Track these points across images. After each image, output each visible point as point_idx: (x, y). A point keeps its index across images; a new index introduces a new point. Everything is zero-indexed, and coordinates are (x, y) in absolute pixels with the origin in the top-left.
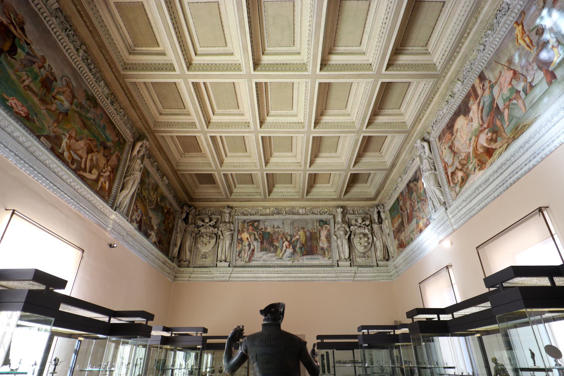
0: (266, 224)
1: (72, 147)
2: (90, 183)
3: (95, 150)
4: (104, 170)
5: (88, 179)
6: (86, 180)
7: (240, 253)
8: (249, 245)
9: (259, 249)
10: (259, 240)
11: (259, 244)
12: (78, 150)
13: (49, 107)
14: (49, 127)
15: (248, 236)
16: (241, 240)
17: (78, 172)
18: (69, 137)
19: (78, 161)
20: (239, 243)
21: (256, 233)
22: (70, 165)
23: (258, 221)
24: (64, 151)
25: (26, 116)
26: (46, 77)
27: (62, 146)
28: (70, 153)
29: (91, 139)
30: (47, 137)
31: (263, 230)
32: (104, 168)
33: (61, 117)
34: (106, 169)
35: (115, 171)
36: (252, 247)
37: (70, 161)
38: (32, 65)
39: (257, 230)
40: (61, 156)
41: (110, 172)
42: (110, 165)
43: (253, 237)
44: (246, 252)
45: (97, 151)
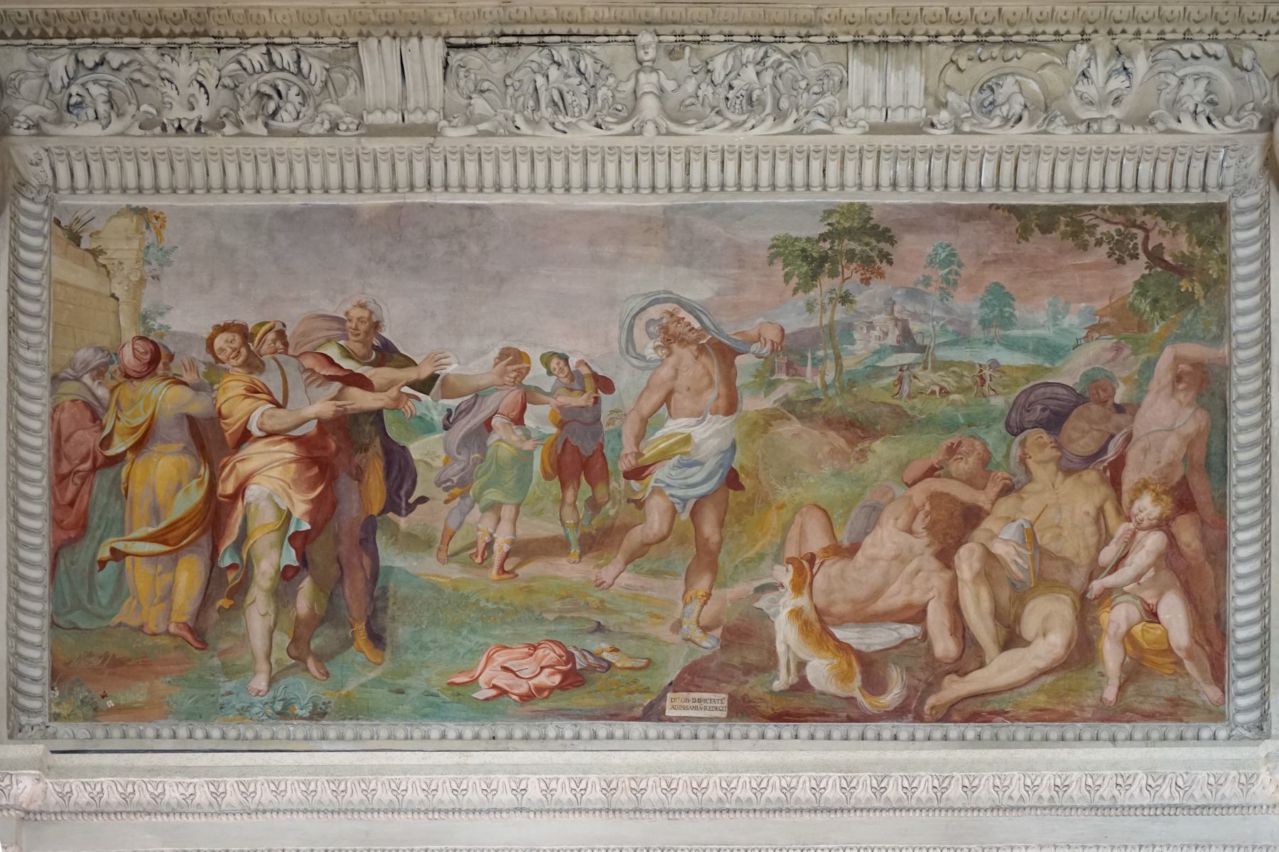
1: (840, 608)
2: (1042, 701)
3: (982, 499)
4: (1108, 554)
5: (1011, 688)
6: (994, 704)
12: (877, 594)
13: (635, 536)
14: (677, 627)
17: (931, 701)
18: (799, 571)
19: (906, 642)
22: (865, 702)
24: (802, 665)
25: (565, 675)
26: (561, 425)
27: (780, 648)
28: (843, 648)
29: (935, 458)
30: (692, 678)
32: (1105, 538)
33: (709, 529)
34: (1122, 529)
35: (1202, 495)
37: (855, 688)
38: (483, 448)
40: (795, 702)
41: (1163, 524)
42: (1143, 487)
45: (1007, 490)
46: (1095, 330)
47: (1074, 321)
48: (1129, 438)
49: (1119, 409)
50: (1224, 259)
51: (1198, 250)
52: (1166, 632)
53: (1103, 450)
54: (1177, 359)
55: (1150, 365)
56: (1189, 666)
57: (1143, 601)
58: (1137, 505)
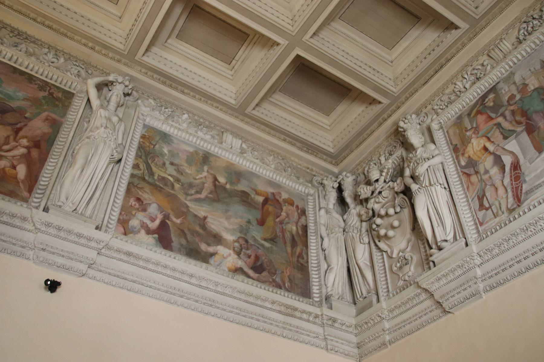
0: (517, 78)
7: (481, 198)
8: (498, 161)
9: (532, 151)
10: (519, 129)
11: (525, 137)
15: (483, 142)
16: (472, 163)
20: (468, 175)
21: (500, 120)
23: (493, 89)
31: (518, 97)
32: (7, 143)
34: (13, 144)
36: (507, 160)
39: (501, 111)
43: (497, 135)
44: (498, 184)
46: (25, 99)
47: (20, 94)
48: (26, 125)
49: (26, 118)
50: (70, 103)
51: (63, 98)
52: (17, 173)
53: (17, 124)
54: (48, 116)
55: (39, 114)
56: (21, 184)
57: (12, 163)
58: (21, 140)
